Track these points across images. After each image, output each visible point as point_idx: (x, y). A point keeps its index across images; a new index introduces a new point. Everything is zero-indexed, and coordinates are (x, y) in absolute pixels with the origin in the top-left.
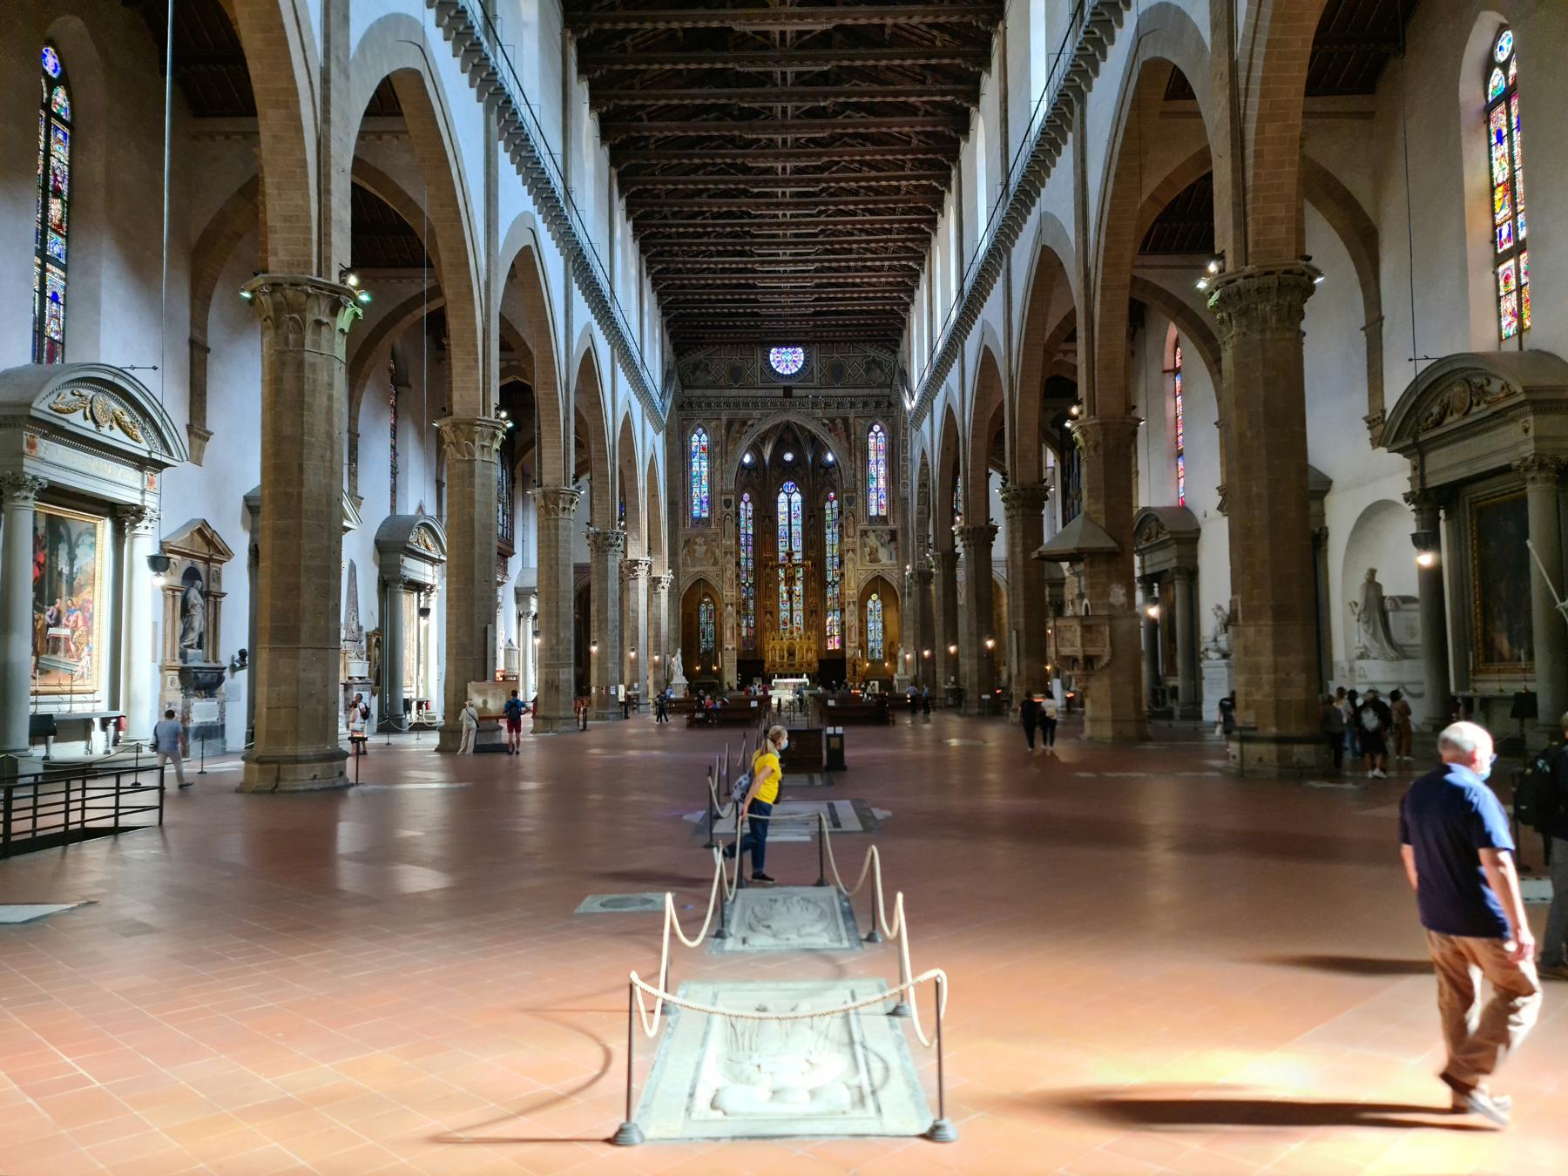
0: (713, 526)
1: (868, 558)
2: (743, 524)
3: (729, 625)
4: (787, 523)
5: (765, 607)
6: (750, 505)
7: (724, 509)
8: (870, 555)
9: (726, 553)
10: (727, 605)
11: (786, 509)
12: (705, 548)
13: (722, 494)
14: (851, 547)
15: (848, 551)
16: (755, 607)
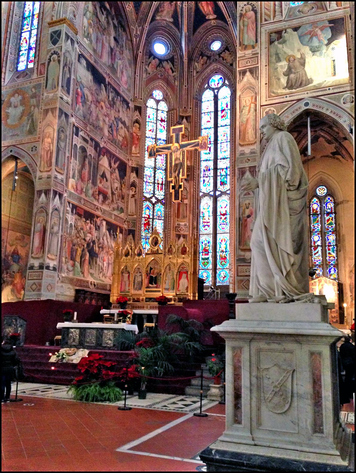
0: (35, 76)
1: (284, 80)
2: (150, 126)
3: (39, 226)
4: (212, 124)
5: (177, 228)
6: (163, 106)
7: (51, 46)
8: (287, 74)
9: (46, 111)
10: (40, 192)
11: (212, 109)
12: (20, 109)
13: (51, 24)
14: (250, 65)
15: (244, 73)
16: (165, 228)
